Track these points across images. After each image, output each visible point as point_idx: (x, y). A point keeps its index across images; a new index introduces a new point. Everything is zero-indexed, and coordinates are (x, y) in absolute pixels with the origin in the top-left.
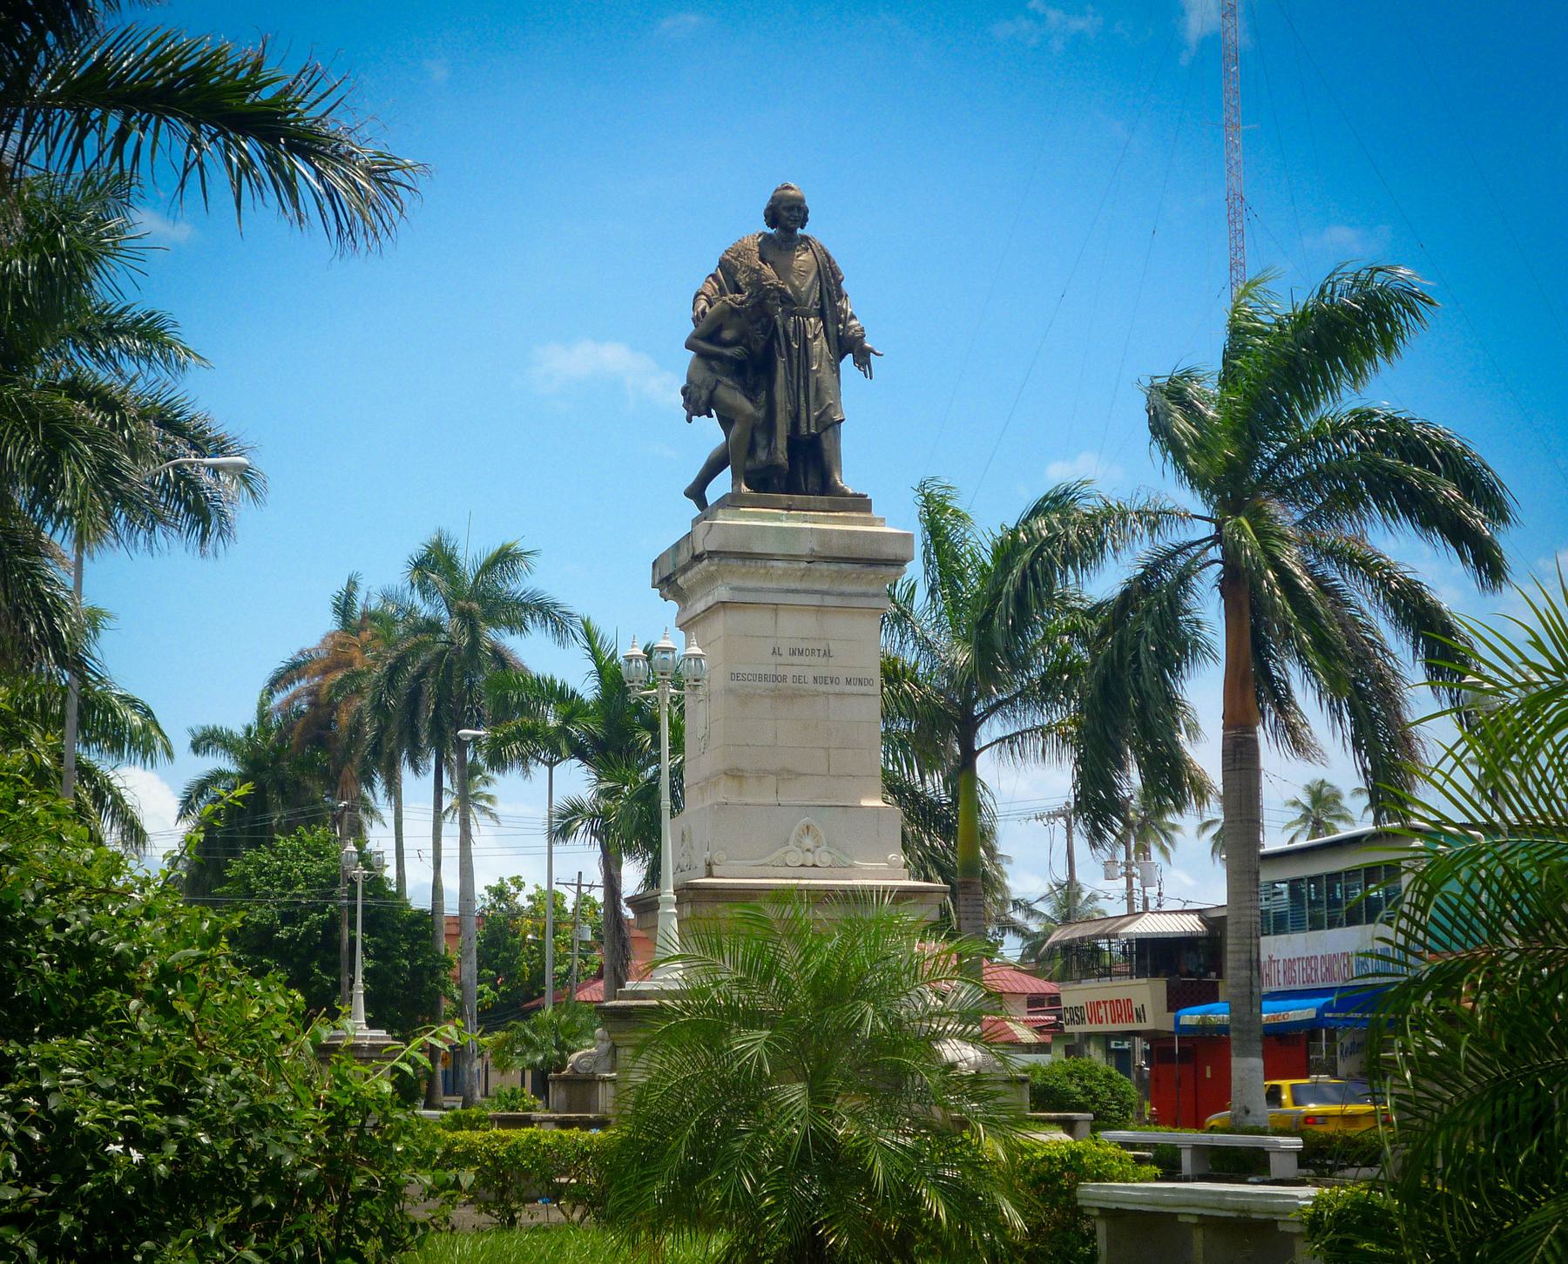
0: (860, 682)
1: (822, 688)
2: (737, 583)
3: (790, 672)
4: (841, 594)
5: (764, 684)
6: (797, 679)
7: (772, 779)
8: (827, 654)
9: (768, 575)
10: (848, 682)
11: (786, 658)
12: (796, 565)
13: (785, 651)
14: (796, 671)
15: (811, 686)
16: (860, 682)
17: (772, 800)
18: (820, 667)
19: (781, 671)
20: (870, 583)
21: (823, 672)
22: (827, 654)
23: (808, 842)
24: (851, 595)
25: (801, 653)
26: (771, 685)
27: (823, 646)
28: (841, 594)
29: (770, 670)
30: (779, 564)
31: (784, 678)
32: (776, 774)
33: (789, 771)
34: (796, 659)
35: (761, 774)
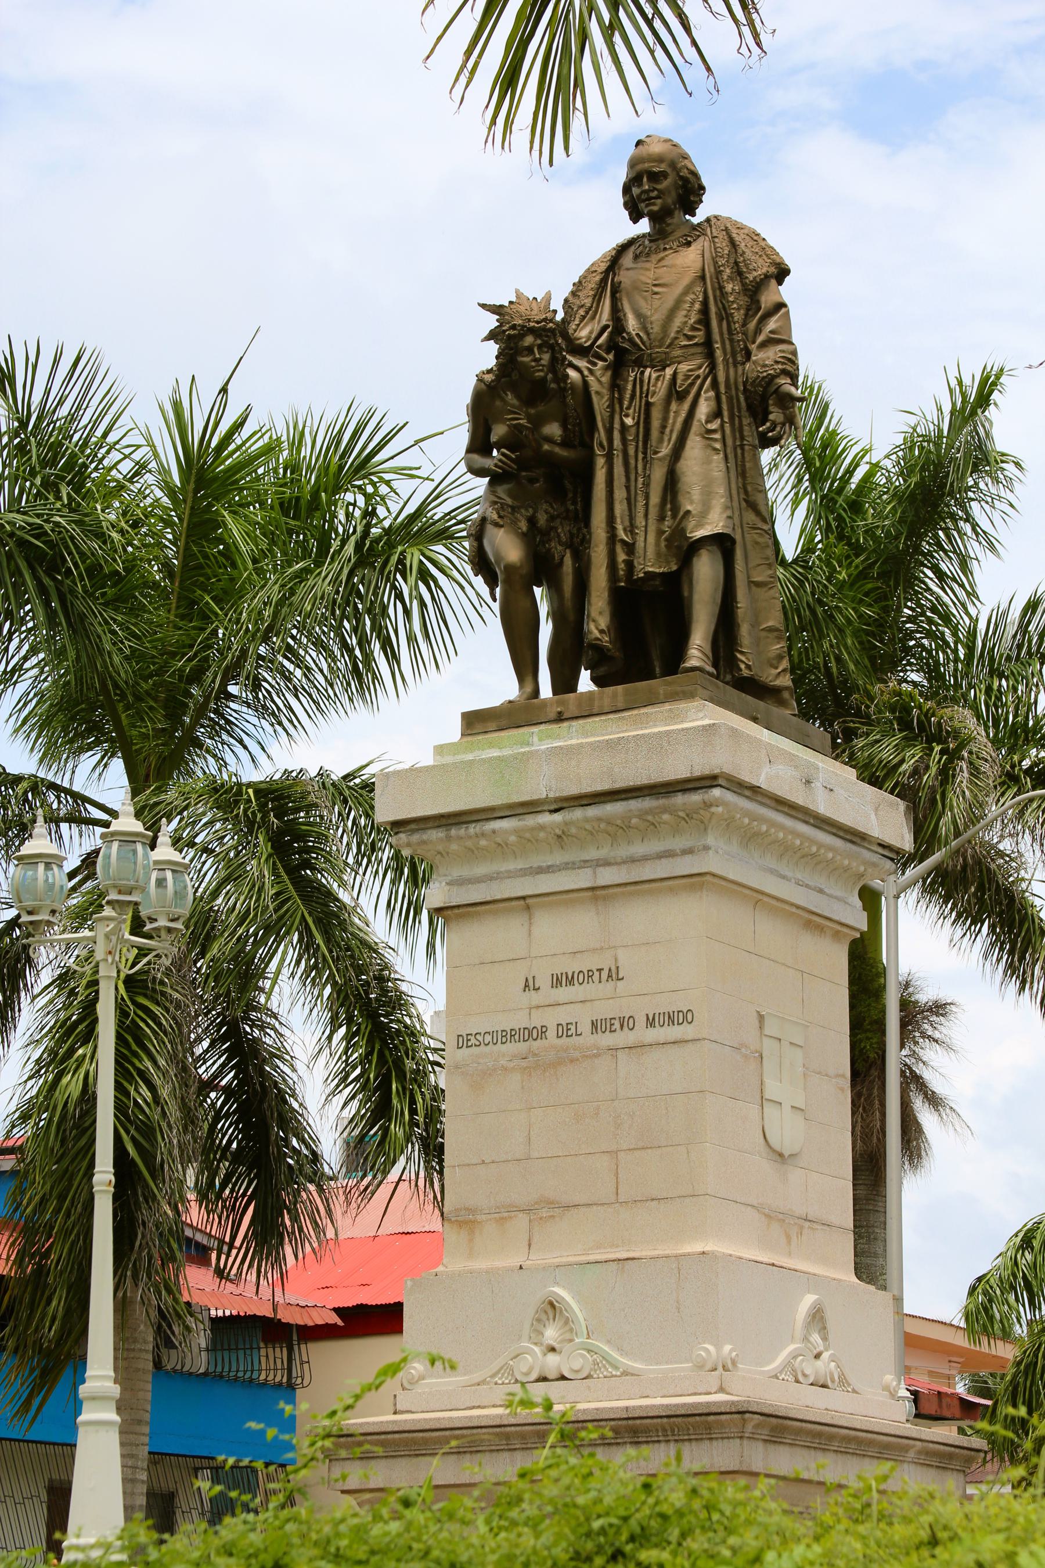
0: (671, 1019)
1: (607, 1040)
2: (456, 872)
3: (551, 1019)
4: (633, 860)
5: (511, 1048)
6: (565, 1030)
7: (522, 1220)
8: (614, 975)
9: (502, 848)
10: (651, 1022)
11: (548, 994)
12: (531, 821)
13: (544, 981)
14: (563, 1015)
15: (588, 1039)
16: (671, 1019)
17: (515, 1261)
18: (600, 1000)
19: (537, 1020)
20: (676, 831)
21: (605, 1010)
22: (614, 975)
23: (551, 1334)
24: (645, 858)
25: (570, 981)
26: (522, 1047)
27: (606, 963)
28: (633, 860)
29: (519, 1021)
30: (504, 824)
31: (543, 1031)
32: (527, 1211)
33: (551, 1203)
34: (564, 993)
35: (505, 1213)
